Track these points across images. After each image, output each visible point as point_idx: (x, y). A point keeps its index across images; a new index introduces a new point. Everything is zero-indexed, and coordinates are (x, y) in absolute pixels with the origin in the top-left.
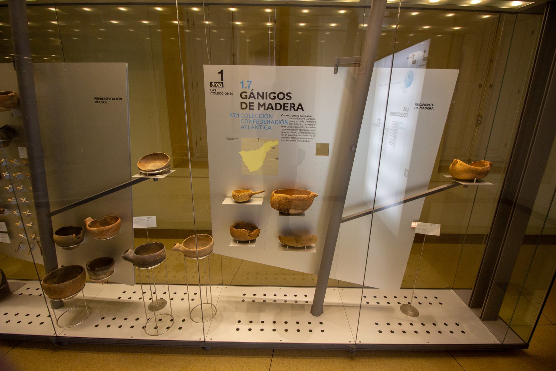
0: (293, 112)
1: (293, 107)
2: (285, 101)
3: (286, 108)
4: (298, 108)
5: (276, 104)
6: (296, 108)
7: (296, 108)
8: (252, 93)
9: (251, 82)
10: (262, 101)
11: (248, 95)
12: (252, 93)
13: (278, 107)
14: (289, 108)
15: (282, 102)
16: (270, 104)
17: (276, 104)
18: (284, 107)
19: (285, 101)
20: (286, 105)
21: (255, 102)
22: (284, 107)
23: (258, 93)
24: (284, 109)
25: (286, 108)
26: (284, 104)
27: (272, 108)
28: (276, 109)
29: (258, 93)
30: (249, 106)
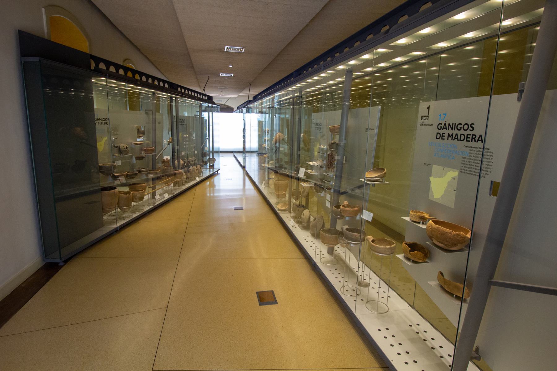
0: (473, 144)
1: (474, 138)
2: (468, 132)
3: (468, 139)
4: (478, 140)
5: (461, 135)
6: (476, 139)
7: (476, 139)
8: (445, 124)
9: (446, 114)
10: (450, 132)
11: (442, 126)
12: (445, 124)
13: (463, 137)
14: (470, 139)
15: (466, 133)
16: (457, 135)
17: (461, 135)
18: (467, 138)
19: (468, 132)
20: (469, 136)
21: (446, 132)
22: (467, 137)
23: (449, 125)
24: (467, 141)
25: (468, 139)
26: (468, 135)
27: (457, 139)
28: (460, 140)
29: (449, 125)
30: (442, 136)
